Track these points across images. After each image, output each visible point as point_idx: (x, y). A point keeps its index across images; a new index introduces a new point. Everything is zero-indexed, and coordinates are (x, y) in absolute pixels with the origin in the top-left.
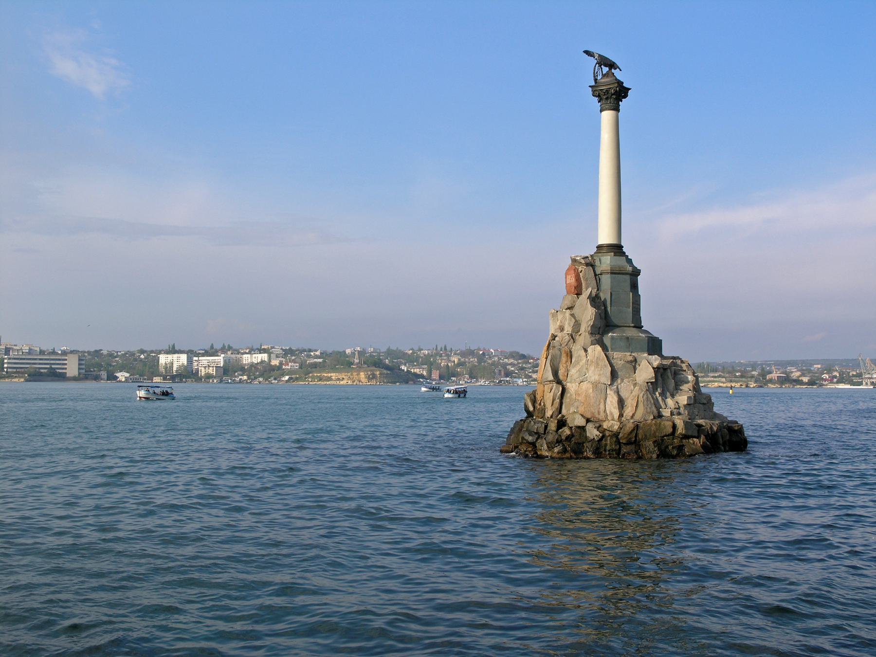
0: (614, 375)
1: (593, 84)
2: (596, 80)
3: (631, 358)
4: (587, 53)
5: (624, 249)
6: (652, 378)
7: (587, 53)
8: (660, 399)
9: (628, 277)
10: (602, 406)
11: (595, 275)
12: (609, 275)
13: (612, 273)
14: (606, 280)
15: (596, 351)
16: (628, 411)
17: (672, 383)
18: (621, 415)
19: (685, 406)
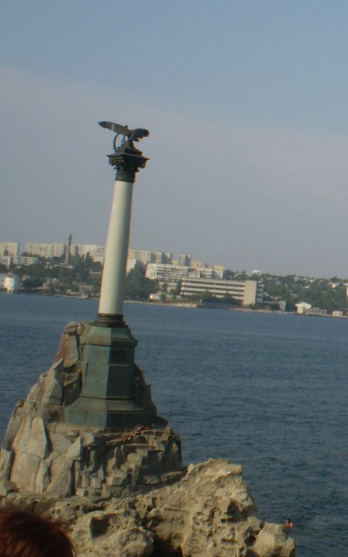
0: (50, 448)
1: (112, 152)
2: (115, 148)
3: (71, 434)
4: (104, 124)
5: (124, 319)
6: (77, 457)
7: (104, 124)
8: (84, 478)
9: (108, 349)
10: (33, 478)
11: (78, 344)
12: (89, 346)
13: (91, 345)
14: (87, 348)
15: (39, 422)
16: (50, 487)
17: (112, 462)
18: (44, 489)
19: (109, 488)
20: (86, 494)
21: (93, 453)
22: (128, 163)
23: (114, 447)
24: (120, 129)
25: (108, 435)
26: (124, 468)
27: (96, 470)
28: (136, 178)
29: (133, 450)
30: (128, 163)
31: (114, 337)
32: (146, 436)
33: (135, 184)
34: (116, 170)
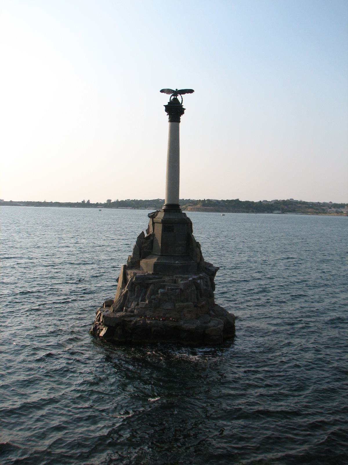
4: (162, 91)
7: (162, 91)
20: (126, 311)
21: (136, 287)
22: (175, 111)
23: (151, 284)
24: (168, 91)
25: (151, 277)
26: (152, 297)
27: (138, 297)
28: (181, 120)
29: (163, 287)
30: (175, 111)
31: (168, 217)
32: (177, 279)
33: (180, 124)
34: (168, 115)
